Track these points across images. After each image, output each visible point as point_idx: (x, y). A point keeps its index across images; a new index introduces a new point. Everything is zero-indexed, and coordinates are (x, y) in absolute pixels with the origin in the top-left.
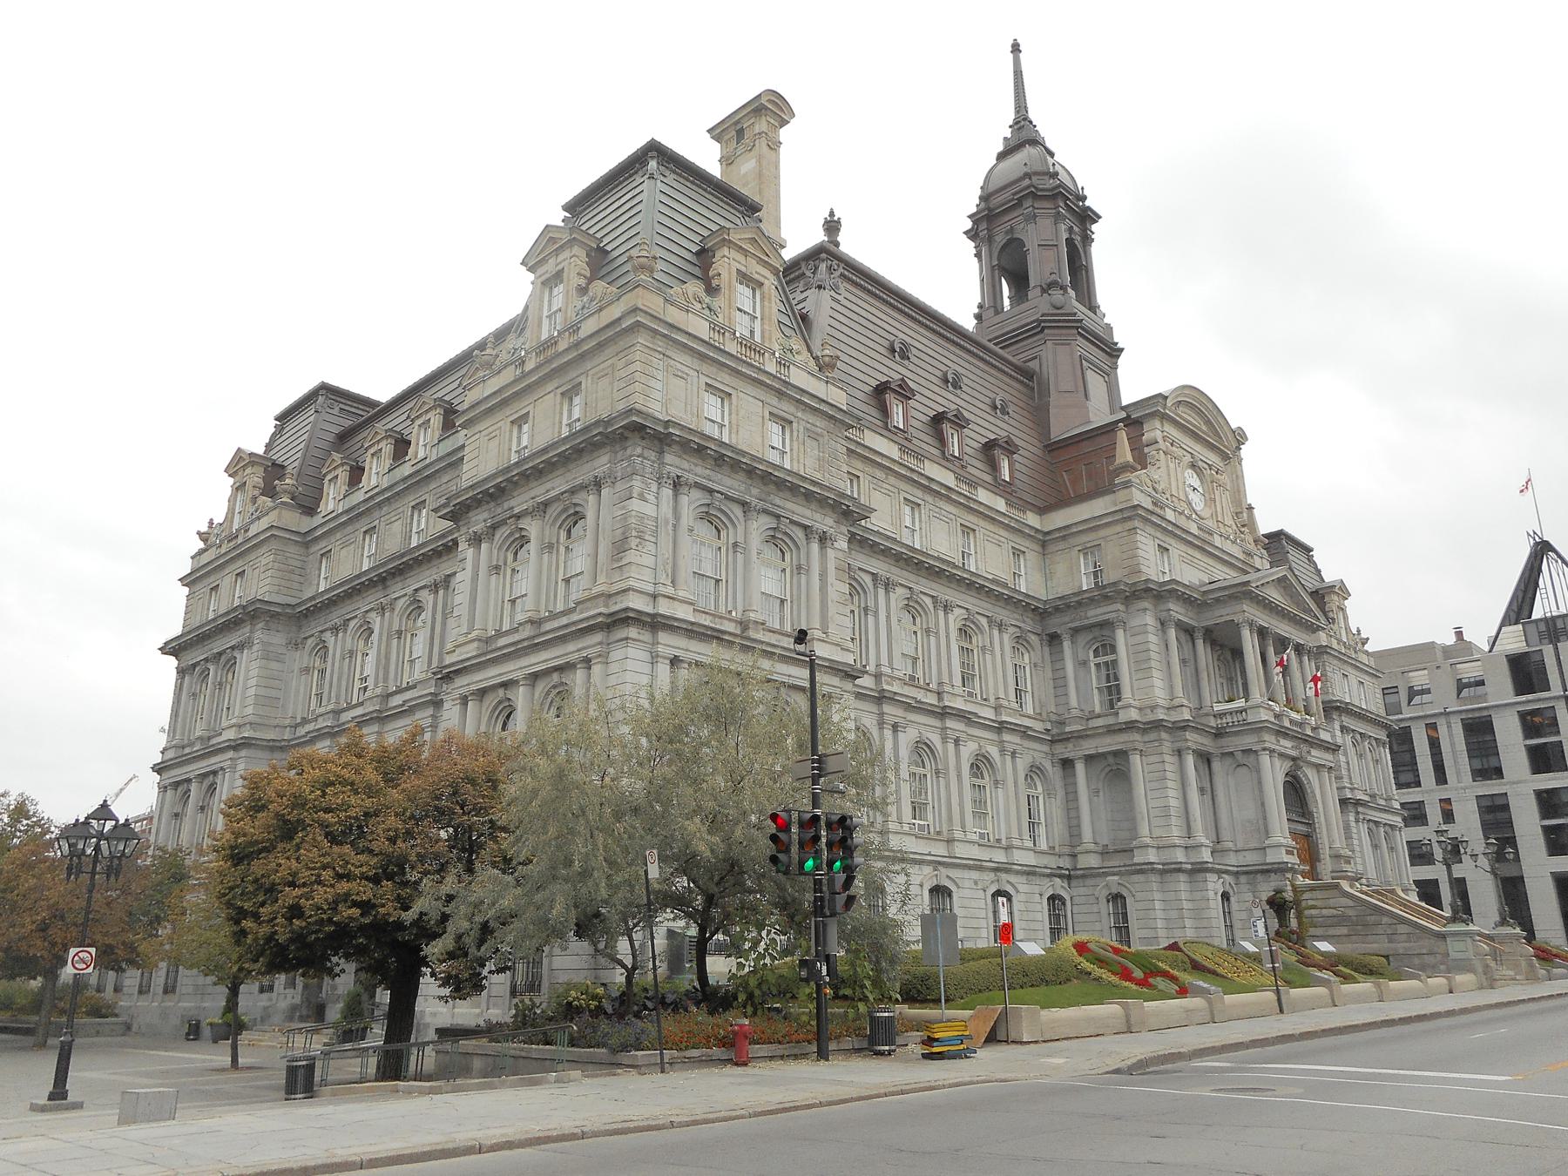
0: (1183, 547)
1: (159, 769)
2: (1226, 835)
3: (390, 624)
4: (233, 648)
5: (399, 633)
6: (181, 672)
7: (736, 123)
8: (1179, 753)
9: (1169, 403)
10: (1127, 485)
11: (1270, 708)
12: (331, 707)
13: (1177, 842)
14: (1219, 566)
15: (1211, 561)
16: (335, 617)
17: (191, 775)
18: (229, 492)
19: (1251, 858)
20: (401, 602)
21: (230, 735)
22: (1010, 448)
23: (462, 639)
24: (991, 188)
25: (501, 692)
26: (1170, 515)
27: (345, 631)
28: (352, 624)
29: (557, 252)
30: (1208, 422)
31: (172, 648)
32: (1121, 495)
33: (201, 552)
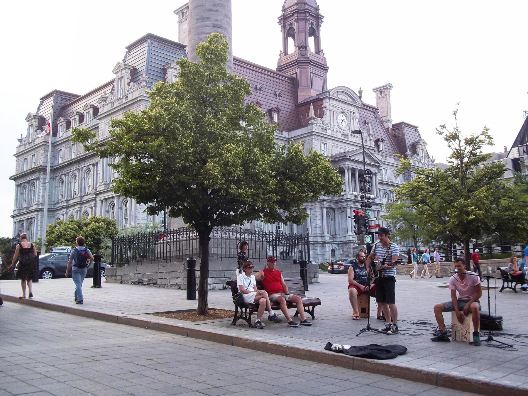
0: (334, 142)
1: (13, 217)
2: (337, 233)
3: (81, 176)
4: (33, 179)
5: (84, 178)
6: (18, 186)
7: (182, 10)
8: (322, 208)
9: (331, 93)
10: (311, 124)
11: (352, 194)
12: (65, 199)
13: (318, 235)
14: (349, 146)
15: (346, 145)
16: (65, 171)
17: (24, 219)
18: (27, 127)
19: (343, 239)
20: (85, 168)
21: (35, 207)
22: (278, 111)
23: (100, 184)
24: (286, 7)
25: (111, 199)
26: (329, 132)
27: (68, 176)
28: (70, 173)
29: (122, 70)
30: (350, 96)
31: (15, 178)
32: (309, 127)
33: (20, 146)
